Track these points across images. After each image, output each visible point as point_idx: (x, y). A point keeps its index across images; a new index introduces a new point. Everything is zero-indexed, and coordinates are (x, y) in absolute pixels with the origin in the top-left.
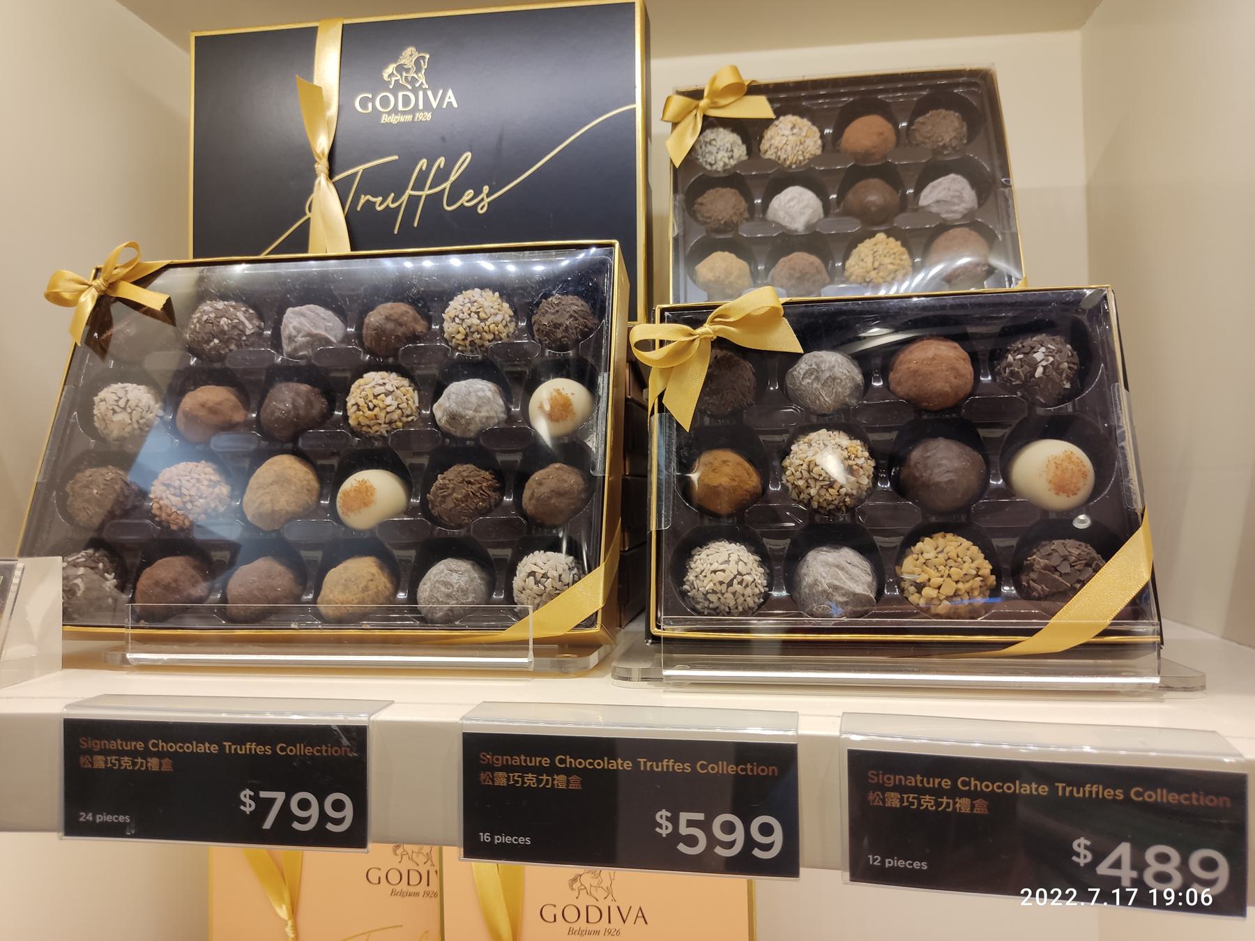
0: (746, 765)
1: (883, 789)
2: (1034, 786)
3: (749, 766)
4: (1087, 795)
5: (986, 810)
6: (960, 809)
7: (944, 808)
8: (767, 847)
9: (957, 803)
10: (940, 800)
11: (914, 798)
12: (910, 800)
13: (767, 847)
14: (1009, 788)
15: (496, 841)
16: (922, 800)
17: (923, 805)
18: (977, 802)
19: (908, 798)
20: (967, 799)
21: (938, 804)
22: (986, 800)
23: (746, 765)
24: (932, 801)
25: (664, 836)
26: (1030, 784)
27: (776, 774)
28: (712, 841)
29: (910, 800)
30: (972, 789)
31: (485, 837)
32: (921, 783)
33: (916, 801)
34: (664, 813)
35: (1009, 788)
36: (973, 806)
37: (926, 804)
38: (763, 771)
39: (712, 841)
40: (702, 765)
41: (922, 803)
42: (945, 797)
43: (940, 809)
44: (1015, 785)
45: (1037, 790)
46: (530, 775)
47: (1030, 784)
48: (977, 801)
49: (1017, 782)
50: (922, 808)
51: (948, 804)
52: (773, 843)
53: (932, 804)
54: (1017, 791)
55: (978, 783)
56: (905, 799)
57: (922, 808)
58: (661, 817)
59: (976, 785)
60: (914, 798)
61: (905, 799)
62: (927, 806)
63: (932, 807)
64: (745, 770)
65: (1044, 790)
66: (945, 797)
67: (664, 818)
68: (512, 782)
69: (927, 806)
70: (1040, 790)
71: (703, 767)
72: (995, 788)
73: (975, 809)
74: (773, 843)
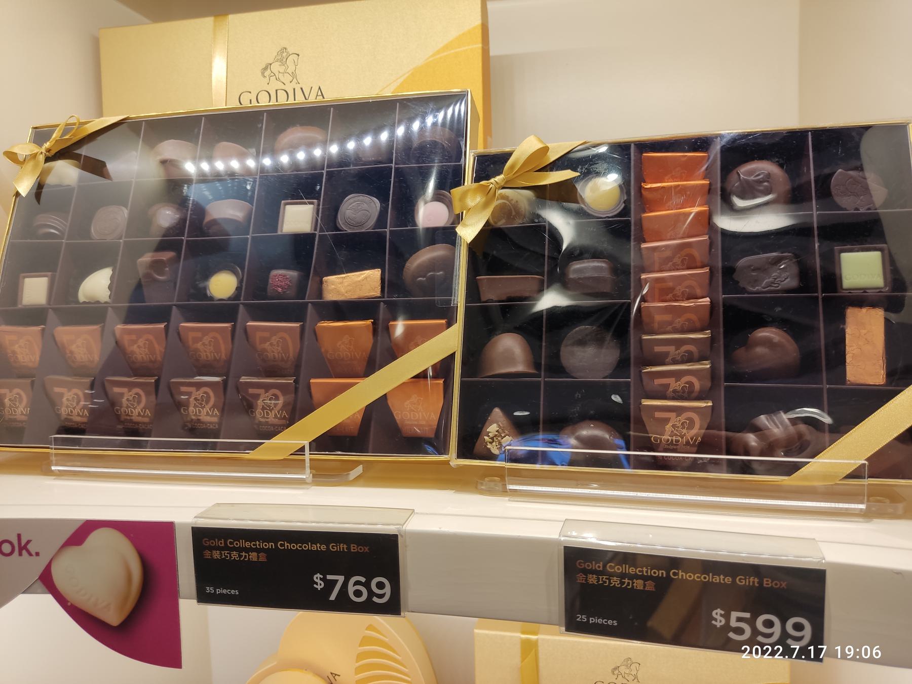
0: (255, 542)
1: (211, 549)
2: (722, 577)
3: (258, 543)
4: (751, 584)
5: (654, 588)
6: (636, 587)
7: (626, 586)
8: (381, 596)
9: (634, 582)
10: (623, 580)
11: (606, 579)
12: (604, 580)
13: (381, 596)
14: (705, 578)
15: (217, 592)
16: (612, 580)
17: (612, 583)
18: (648, 583)
19: (224, 553)
20: (641, 580)
21: (240, 556)
22: (654, 582)
23: (255, 542)
24: (618, 581)
25: (319, 589)
26: (719, 576)
27: (274, 547)
28: (371, 594)
29: (604, 580)
30: (286, 548)
31: (210, 590)
32: (646, 573)
33: (229, 555)
34: (319, 575)
35: (305, 547)
36: (645, 585)
37: (614, 583)
38: (361, 549)
39: (371, 594)
40: (230, 542)
41: (612, 582)
42: (626, 579)
43: (623, 586)
44: (709, 576)
45: (724, 580)
46: (235, 552)
47: (719, 576)
48: (648, 582)
49: (711, 574)
50: (611, 585)
51: (245, 556)
52: (385, 593)
53: (618, 583)
54: (711, 580)
55: (684, 574)
56: (601, 579)
57: (611, 585)
58: (317, 578)
59: (682, 575)
60: (606, 579)
61: (601, 579)
62: (615, 584)
63: (618, 584)
64: (256, 545)
65: (728, 580)
66: (626, 579)
67: (319, 578)
68: (223, 557)
69: (615, 584)
70: (726, 580)
71: (281, 545)
72: (696, 578)
73: (647, 587)
74: (385, 593)
